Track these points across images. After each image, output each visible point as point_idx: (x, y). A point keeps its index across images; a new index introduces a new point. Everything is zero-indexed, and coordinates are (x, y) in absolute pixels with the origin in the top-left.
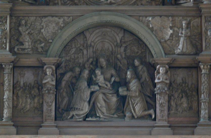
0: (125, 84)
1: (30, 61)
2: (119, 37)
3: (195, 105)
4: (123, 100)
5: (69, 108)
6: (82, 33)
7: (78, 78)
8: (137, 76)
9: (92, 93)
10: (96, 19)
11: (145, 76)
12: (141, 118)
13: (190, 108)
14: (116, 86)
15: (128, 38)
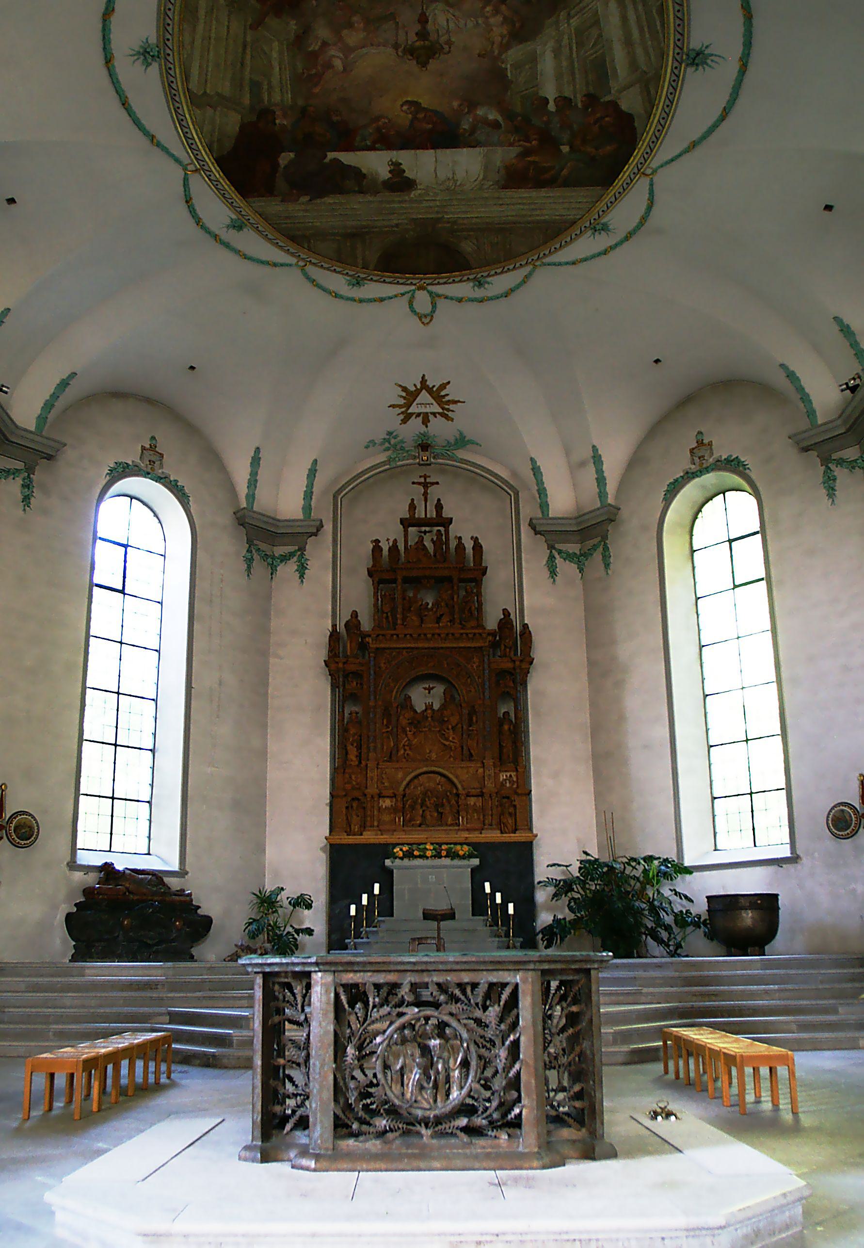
0: (443, 805)
1: (390, 792)
2: (438, 778)
3: (481, 817)
4: (441, 814)
5: (411, 820)
6: (416, 777)
7: (415, 802)
8: (449, 802)
9: (423, 811)
10: (425, 769)
11: (453, 802)
12: (451, 825)
13: (479, 819)
14: (437, 806)
15: (443, 779)
